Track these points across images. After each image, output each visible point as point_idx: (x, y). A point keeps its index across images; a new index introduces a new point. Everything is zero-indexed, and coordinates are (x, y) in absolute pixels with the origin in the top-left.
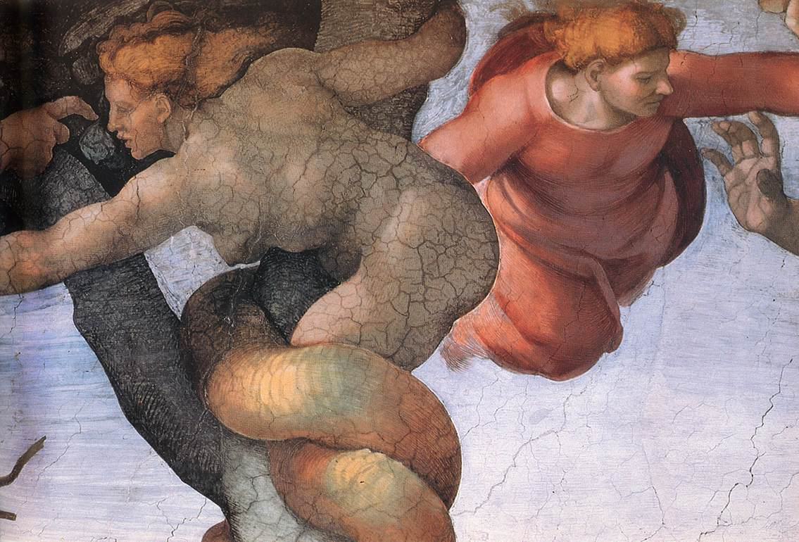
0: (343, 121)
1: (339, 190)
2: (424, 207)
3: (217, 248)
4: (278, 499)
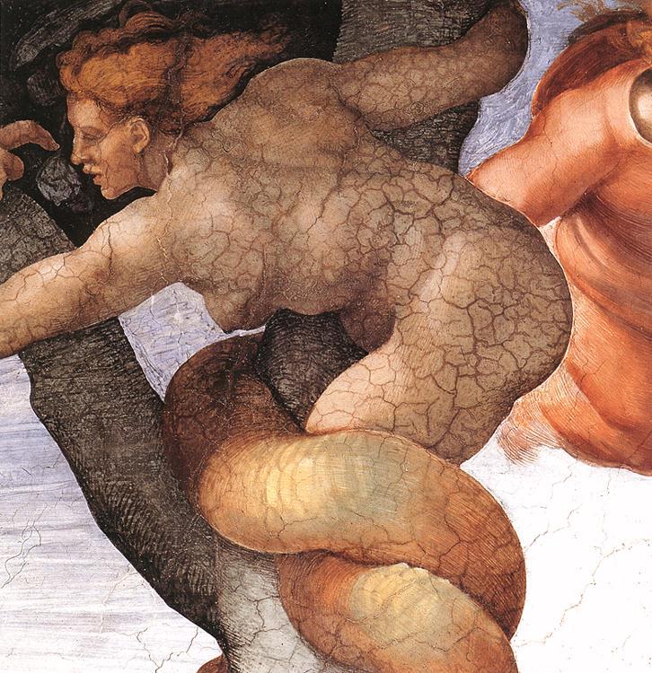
0: (368, 149)
2: (475, 255)
3: (210, 311)
4: (291, 627)
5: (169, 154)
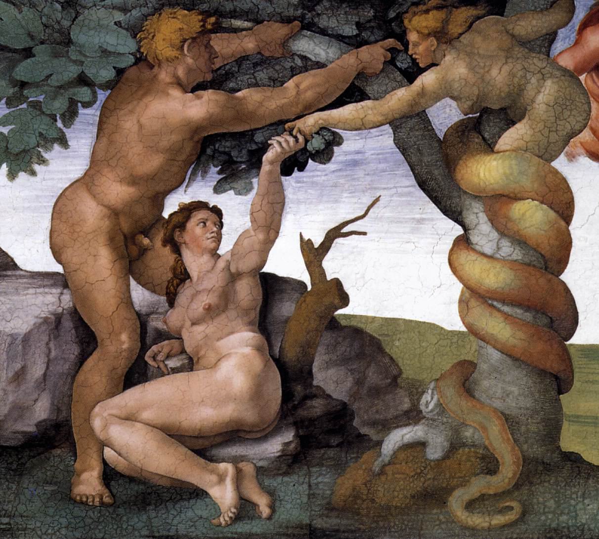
0: (517, 49)
1: (516, 80)
2: (556, 87)
5: (444, 51)
